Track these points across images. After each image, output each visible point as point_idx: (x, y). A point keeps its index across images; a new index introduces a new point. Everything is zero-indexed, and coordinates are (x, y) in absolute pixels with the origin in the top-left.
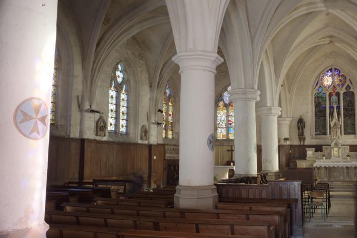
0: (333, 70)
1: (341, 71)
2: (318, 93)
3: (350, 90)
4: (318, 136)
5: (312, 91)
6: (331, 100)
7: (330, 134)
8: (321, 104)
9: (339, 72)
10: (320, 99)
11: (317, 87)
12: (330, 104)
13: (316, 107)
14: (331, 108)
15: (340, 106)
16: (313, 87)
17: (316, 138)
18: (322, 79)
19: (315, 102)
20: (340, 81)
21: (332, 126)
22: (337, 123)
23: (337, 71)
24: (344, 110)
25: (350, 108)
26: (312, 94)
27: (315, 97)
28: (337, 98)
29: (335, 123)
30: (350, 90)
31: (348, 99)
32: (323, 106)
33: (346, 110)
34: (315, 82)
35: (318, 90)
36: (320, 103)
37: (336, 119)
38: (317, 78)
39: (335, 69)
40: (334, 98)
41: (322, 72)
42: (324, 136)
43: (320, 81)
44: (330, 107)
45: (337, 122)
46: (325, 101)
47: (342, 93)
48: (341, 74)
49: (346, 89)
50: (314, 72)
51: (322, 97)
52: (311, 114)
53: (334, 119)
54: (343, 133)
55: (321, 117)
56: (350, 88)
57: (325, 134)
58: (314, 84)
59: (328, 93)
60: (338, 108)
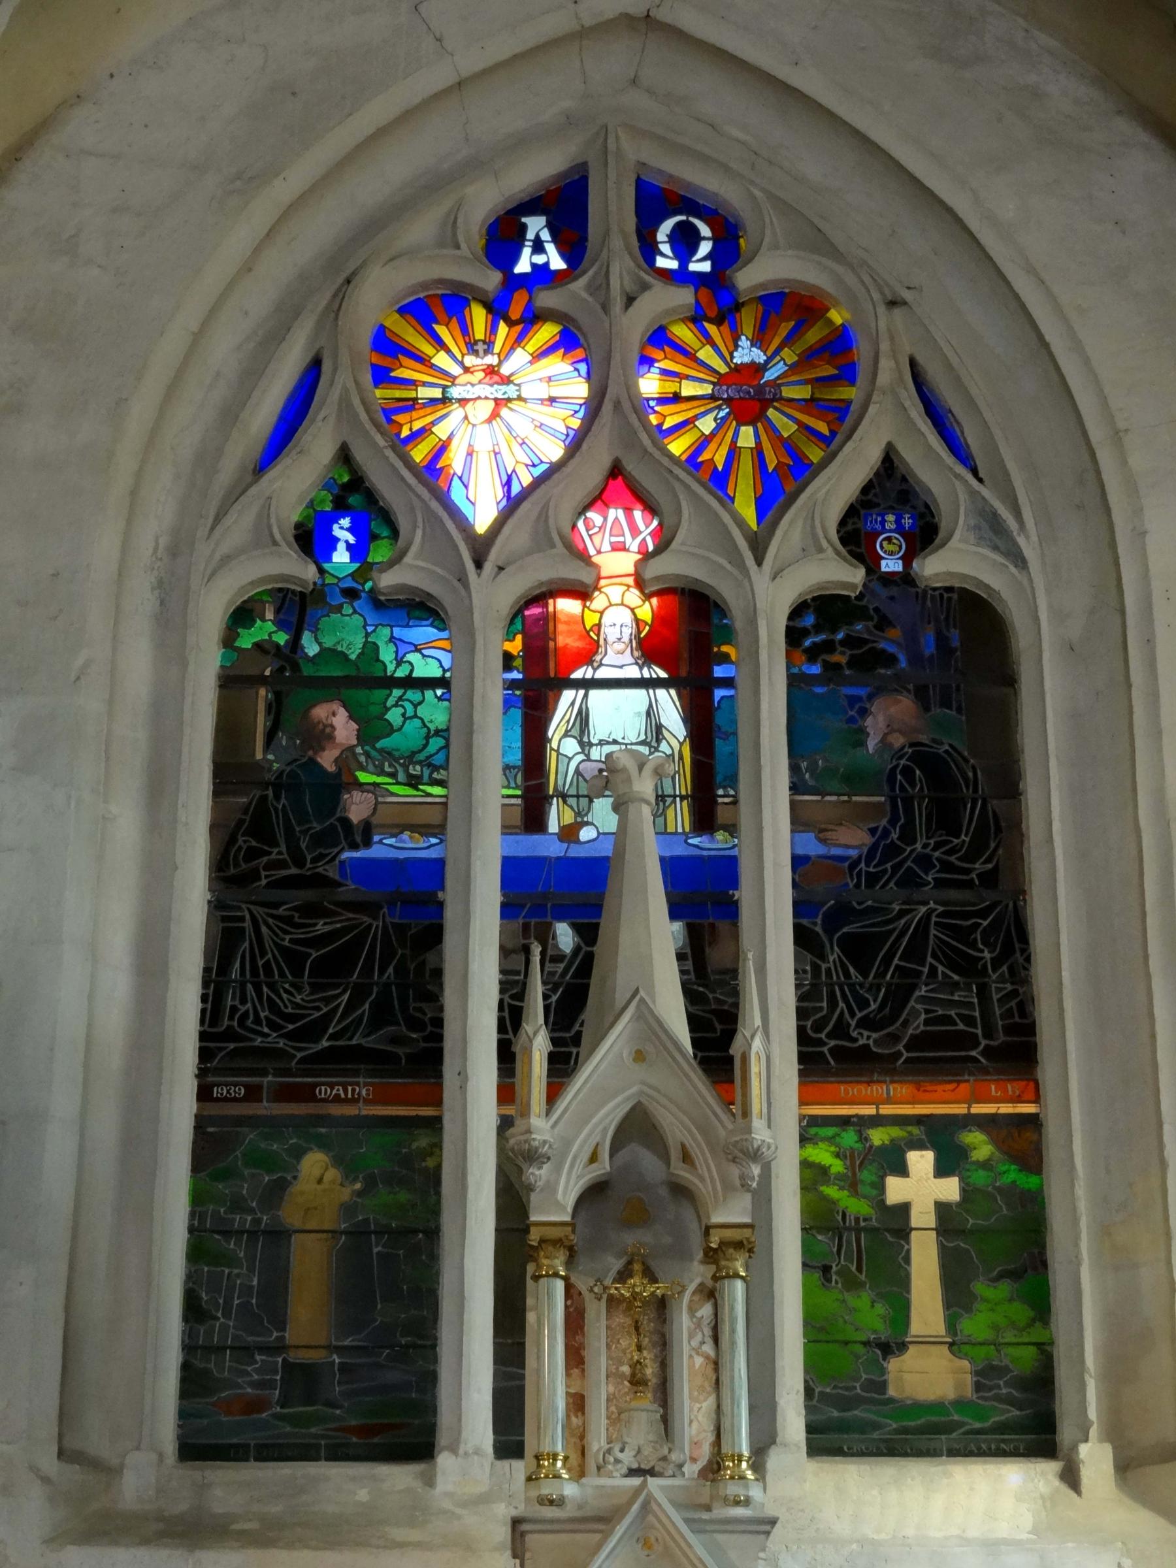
0: (612, 209)
1: (762, 226)
2: (298, 607)
3: (933, 568)
4: (231, 1487)
5: (178, 548)
6: (563, 746)
7: (509, 1445)
8: (357, 808)
9: (727, 252)
10: (344, 729)
11: (299, 480)
12: (532, 816)
13: (230, 870)
14: (559, 896)
15: (726, 870)
16: (207, 459)
17: (192, 1530)
18: (386, 345)
19: (229, 773)
20: (745, 397)
21: (557, 1197)
22: (675, 1127)
23: (685, 242)
24: (803, 938)
25: (929, 905)
26: (170, 620)
27: (231, 682)
28: (669, 707)
29: (637, 1127)
30: (933, 568)
31: (889, 722)
32: (384, 848)
33: (859, 951)
34: (252, 374)
35: (312, 540)
36: (338, 784)
37: (652, 1028)
38: (272, 338)
39: (654, 201)
40: (620, 715)
41: (371, 230)
42: (398, 1477)
43: (344, 381)
44: (514, 872)
45: (680, 1093)
46: (434, 761)
47: (767, 602)
48: (749, 278)
49: (855, 537)
50: (248, 182)
51: (365, 682)
52: (118, 984)
53: (607, 1058)
54: (793, 1421)
55: (344, 1060)
56: (924, 535)
57: (406, 1433)
58: (230, 416)
59: (493, 597)
60: (705, 897)
